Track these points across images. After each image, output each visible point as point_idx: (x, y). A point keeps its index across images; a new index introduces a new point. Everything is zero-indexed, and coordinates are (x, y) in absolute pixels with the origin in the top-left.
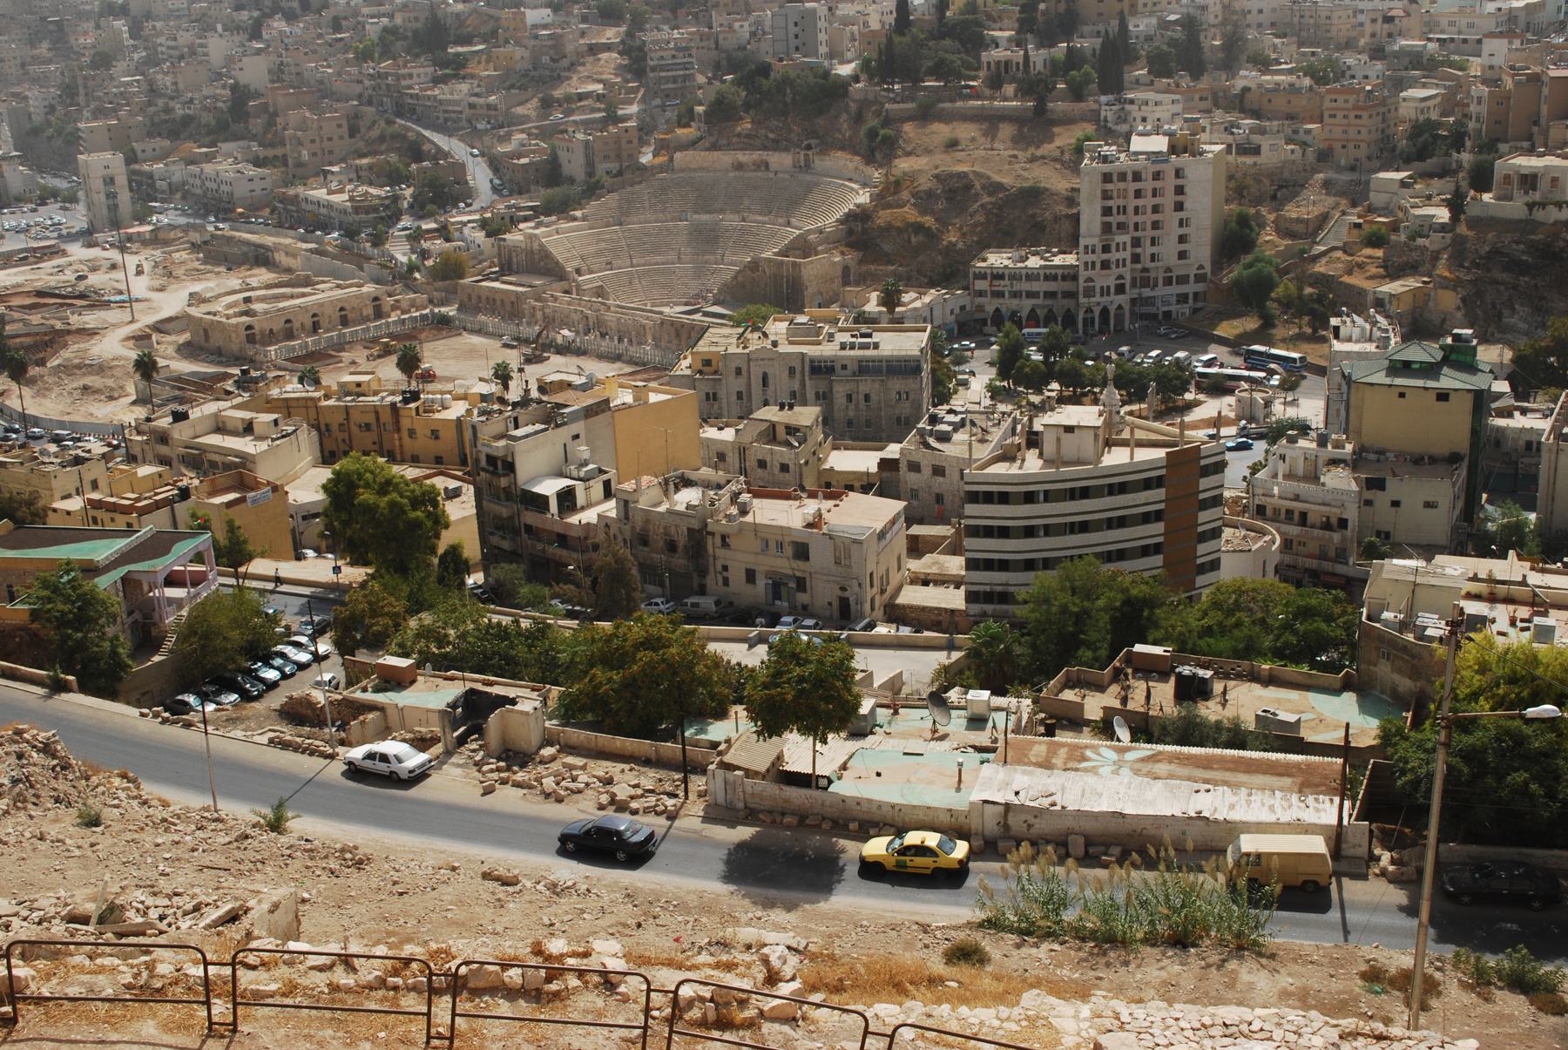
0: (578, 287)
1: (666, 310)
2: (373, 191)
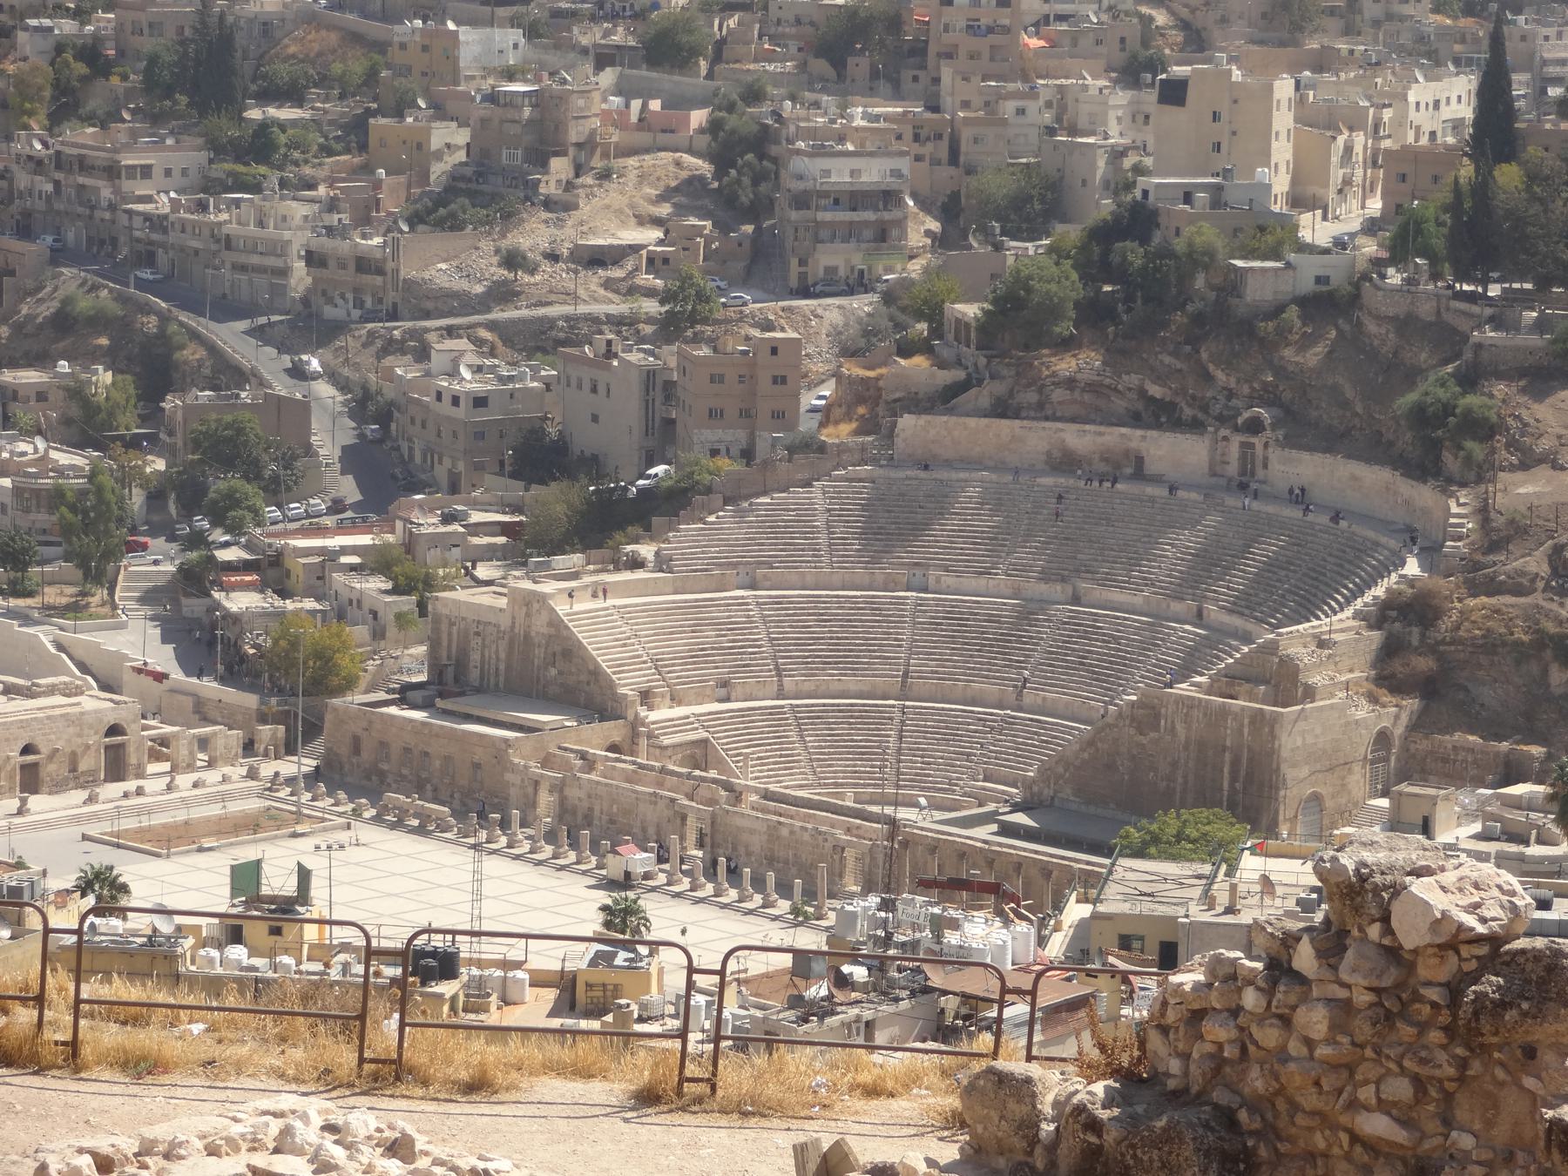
0: (650, 736)
1: (904, 814)
2: (63, 458)
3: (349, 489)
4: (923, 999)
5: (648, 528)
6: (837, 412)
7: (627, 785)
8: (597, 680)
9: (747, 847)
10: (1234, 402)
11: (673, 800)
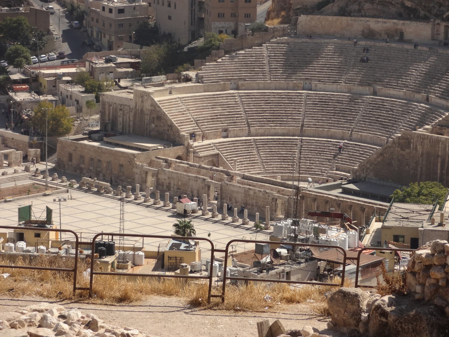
0: (194, 152)
1: (302, 185)
3: (66, 48)
4: (311, 263)
5: (193, 64)
6: (273, 14)
7: (185, 173)
8: (172, 129)
9: (235, 199)
10: (442, 8)
11: (204, 180)
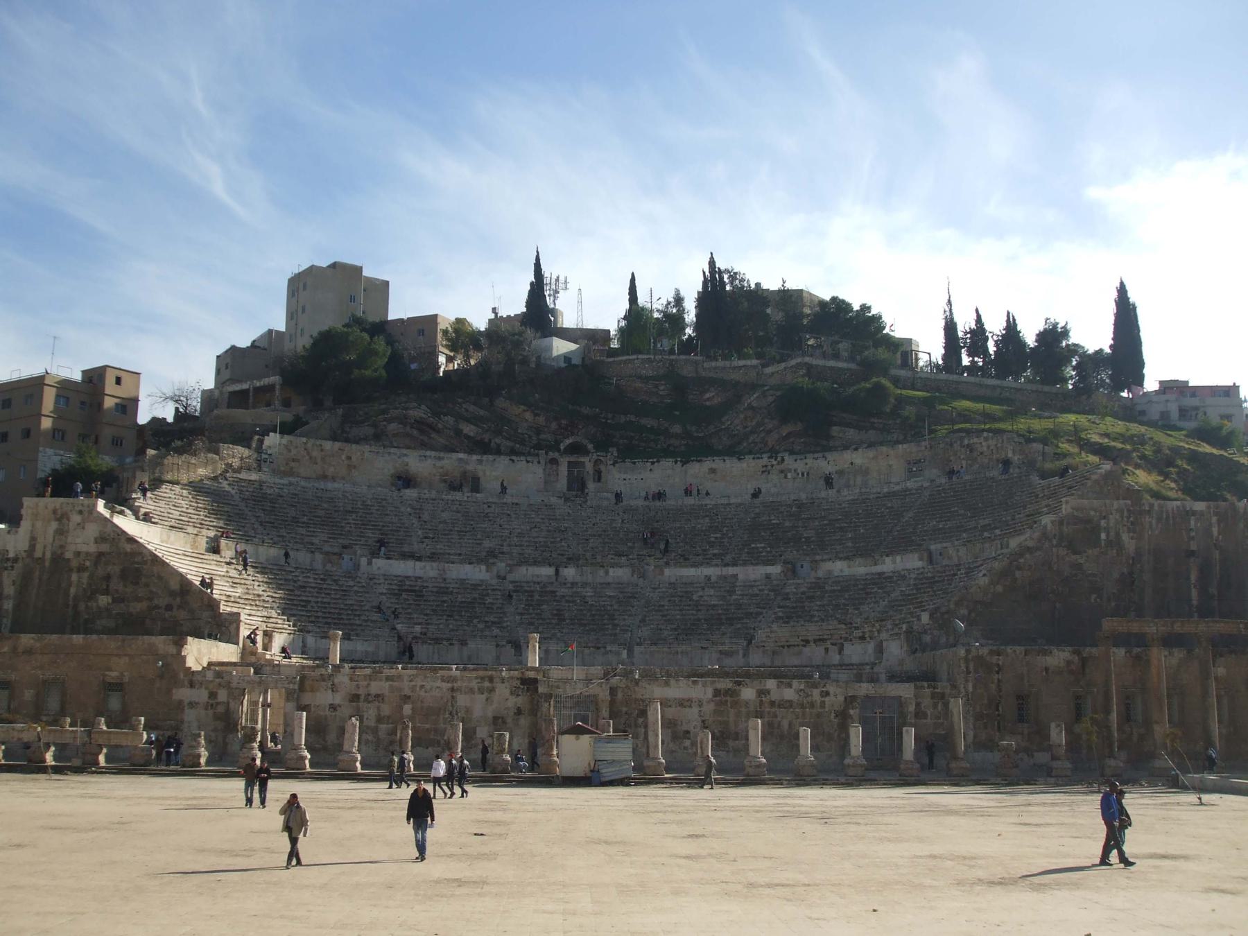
10: (542, 436)
